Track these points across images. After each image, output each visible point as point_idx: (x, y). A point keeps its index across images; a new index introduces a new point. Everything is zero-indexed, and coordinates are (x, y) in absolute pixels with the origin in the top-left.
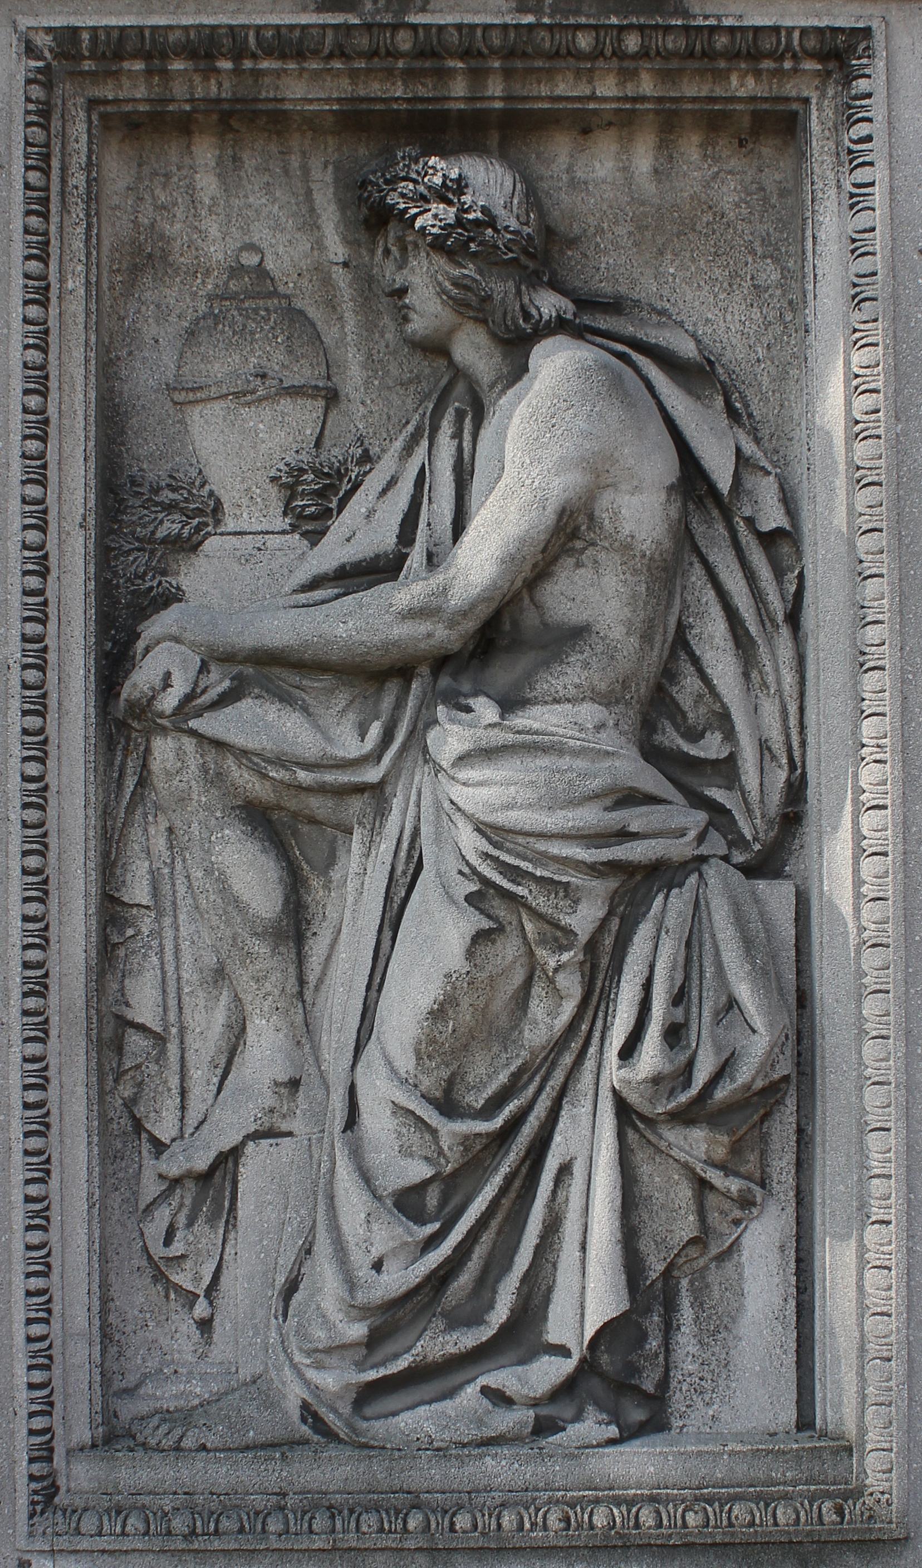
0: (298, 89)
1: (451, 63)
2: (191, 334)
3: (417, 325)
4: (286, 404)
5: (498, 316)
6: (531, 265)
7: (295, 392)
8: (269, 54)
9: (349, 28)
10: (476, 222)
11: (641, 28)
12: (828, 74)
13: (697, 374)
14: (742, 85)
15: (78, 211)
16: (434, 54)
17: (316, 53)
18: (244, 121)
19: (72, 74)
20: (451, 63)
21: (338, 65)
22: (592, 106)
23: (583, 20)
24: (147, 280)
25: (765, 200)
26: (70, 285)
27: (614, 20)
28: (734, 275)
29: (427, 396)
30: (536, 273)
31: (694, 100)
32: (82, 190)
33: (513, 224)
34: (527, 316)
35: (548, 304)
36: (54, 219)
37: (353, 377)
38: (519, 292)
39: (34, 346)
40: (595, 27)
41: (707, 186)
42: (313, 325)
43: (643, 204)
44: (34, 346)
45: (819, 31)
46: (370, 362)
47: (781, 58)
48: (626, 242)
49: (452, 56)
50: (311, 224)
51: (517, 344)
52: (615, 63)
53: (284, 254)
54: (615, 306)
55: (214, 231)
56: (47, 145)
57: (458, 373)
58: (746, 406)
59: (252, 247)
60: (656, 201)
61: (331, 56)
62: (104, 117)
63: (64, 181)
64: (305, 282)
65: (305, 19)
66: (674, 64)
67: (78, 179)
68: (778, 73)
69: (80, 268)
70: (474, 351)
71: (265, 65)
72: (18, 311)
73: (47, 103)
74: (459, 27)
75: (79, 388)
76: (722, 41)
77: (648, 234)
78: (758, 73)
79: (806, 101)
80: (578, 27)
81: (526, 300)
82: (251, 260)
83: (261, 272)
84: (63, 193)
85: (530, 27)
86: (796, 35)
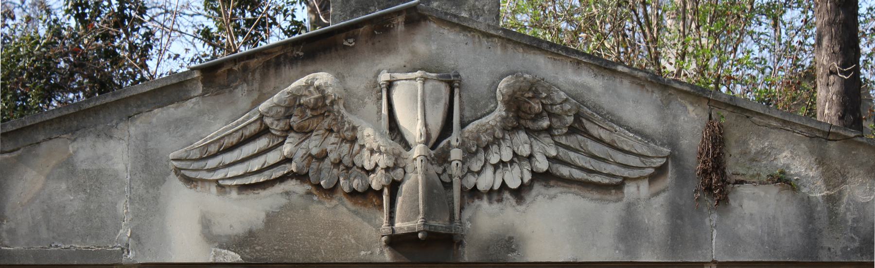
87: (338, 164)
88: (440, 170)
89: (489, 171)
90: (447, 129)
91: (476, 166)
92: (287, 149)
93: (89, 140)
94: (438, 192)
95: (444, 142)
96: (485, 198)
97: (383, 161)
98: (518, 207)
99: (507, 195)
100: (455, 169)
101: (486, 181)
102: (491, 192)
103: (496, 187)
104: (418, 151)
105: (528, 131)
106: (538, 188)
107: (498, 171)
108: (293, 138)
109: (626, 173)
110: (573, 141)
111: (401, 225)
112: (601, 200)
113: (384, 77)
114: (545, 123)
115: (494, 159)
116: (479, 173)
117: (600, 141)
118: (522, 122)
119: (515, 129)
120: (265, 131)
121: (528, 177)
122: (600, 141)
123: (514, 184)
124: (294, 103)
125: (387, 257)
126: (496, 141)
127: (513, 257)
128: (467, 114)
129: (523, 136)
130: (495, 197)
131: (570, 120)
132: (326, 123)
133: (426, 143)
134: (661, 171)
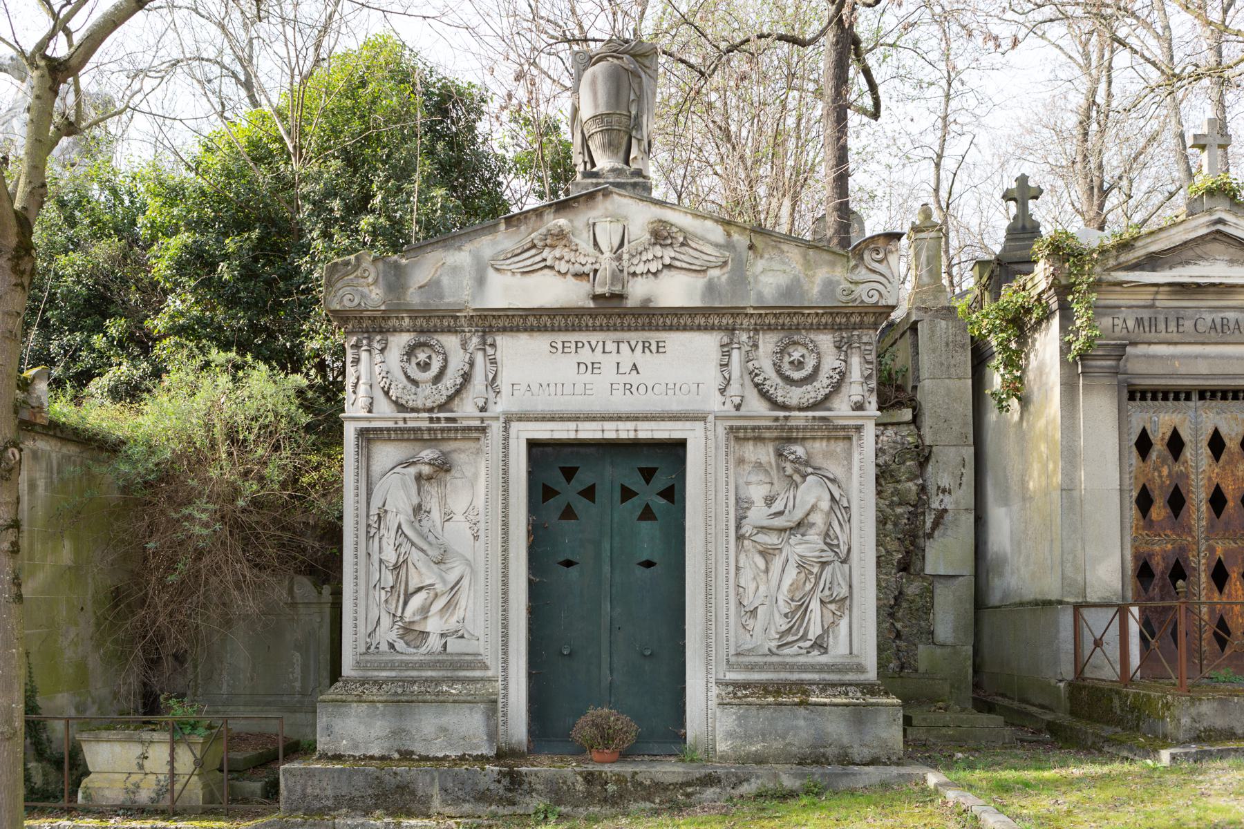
0: (767, 435)
18: (759, 439)
35: (810, 470)
37: (775, 481)
51: (804, 477)
54: (819, 469)
70: (797, 477)
87: (568, 262)
89: (642, 264)
90: (622, 244)
91: (635, 261)
92: (544, 255)
93: (451, 251)
94: (618, 275)
97: (591, 260)
100: (625, 263)
101: (641, 268)
104: (608, 254)
106: (665, 271)
108: (547, 250)
111: (599, 291)
113: (591, 221)
114: (669, 241)
115: (644, 258)
119: (655, 244)
120: (534, 246)
121: (660, 267)
123: (653, 270)
124: (549, 233)
125: (592, 305)
127: (652, 305)
128: (632, 238)
129: (658, 247)
131: (681, 239)
132: (564, 242)
134: (725, 263)
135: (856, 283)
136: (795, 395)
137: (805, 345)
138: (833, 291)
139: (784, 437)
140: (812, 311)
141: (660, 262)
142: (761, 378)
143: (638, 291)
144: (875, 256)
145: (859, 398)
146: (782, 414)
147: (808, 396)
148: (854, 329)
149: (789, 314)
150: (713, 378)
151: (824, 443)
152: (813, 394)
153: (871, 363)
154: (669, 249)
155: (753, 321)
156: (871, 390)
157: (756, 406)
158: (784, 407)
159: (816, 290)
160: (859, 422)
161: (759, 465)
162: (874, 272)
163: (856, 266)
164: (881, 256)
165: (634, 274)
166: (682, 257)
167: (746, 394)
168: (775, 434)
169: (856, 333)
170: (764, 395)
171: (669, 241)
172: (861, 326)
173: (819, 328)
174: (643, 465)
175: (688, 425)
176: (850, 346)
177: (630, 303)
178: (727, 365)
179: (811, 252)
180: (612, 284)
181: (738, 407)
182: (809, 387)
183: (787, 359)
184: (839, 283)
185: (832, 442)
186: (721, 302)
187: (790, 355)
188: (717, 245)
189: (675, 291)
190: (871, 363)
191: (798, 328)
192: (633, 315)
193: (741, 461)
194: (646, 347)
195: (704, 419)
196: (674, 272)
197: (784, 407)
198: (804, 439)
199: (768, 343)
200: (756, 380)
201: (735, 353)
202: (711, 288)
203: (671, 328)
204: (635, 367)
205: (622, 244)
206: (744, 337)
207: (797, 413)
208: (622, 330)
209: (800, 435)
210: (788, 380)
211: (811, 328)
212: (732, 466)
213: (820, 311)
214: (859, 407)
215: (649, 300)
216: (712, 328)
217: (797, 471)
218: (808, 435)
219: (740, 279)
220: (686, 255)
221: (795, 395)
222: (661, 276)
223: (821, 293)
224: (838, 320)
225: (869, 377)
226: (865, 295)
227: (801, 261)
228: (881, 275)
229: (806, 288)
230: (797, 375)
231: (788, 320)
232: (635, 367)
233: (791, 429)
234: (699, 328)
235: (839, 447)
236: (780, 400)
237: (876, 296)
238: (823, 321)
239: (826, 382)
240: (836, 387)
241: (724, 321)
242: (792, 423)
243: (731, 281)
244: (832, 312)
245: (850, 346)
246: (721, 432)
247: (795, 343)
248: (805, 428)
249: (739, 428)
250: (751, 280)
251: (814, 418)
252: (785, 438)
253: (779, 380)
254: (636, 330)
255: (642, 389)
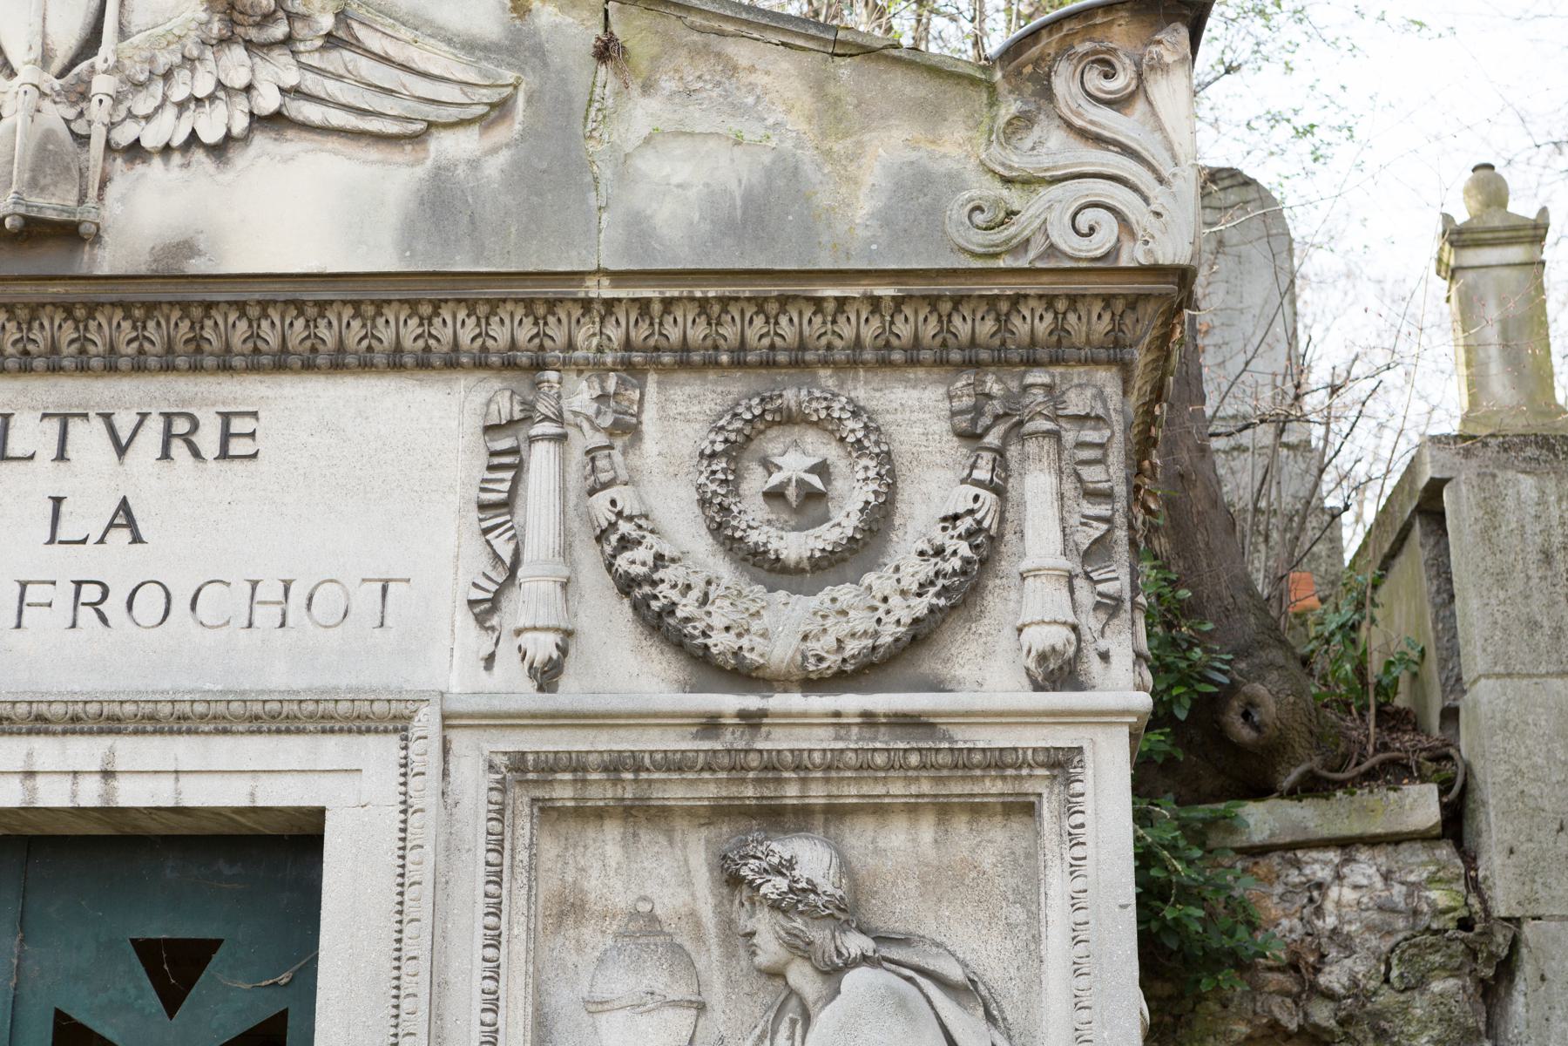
1: (786, 775)
2: (601, 960)
3: (762, 959)
4: (669, 1013)
5: (819, 954)
6: (843, 917)
7: (675, 1004)
8: (658, 768)
9: (715, 752)
10: (804, 890)
11: (920, 750)
12: (1055, 777)
13: (965, 991)
14: (993, 787)
15: (522, 878)
16: (774, 768)
17: (691, 768)
18: (641, 814)
19: (520, 782)
20: (786, 775)
21: (706, 775)
22: (887, 800)
23: (878, 745)
24: (570, 921)
25: (1015, 861)
26: (516, 931)
27: (902, 745)
28: (993, 916)
29: (770, 1007)
30: (847, 921)
31: (960, 796)
32: (525, 863)
33: (830, 890)
34: (839, 954)
35: (856, 943)
36: (505, 885)
37: (716, 994)
38: (834, 937)
39: (491, 978)
40: (888, 750)
41: (973, 851)
42: (689, 956)
43: (927, 865)
44: (491, 978)
45: (1047, 749)
46: (730, 982)
47: (1020, 767)
48: (914, 893)
49: (787, 770)
50: (687, 882)
51: (833, 973)
52: (902, 773)
53: (668, 901)
54: (905, 941)
55: (619, 886)
56: (502, 833)
57: (792, 992)
58: (1001, 1011)
59: (644, 899)
60: (936, 863)
61: (702, 769)
62: (541, 809)
63: (513, 858)
64: (683, 923)
65: (684, 746)
66: (945, 773)
67: (523, 856)
68: (1018, 778)
69: (523, 919)
70: (802, 977)
71: (656, 776)
72: (479, 952)
73: (502, 803)
74: (792, 751)
75: (520, 1005)
76: (977, 757)
77: (930, 888)
78: (1004, 778)
79: (1040, 795)
80: (875, 750)
81: (839, 942)
82: (644, 907)
83: (652, 918)
84: (512, 866)
85: (842, 751)
86: (1030, 753)
88: (71, 113)
89: (170, 112)
90: (91, 43)
91: (143, 104)
95: (83, 66)
96: (157, 162)
98: (220, 178)
99: (199, 155)
100: (98, 112)
101: (164, 129)
102: (167, 149)
103: (177, 142)
105: (249, 45)
106: (261, 141)
107: (186, 114)
109: (433, 113)
110: (337, 60)
112: (384, 162)
114: (279, 31)
115: (179, 93)
116: (148, 118)
117: (385, 60)
118: (239, 30)
121: (240, 124)
122: (385, 60)
123: (211, 135)
126: (189, 61)
127: (196, 266)
129: (238, 53)
130: (177, 158)
131: (327, 22)
133: (45, 59)
134: (501, 108)
135: (1028, 182)
136: (783, 627)
137: (827, 426)
138: (934, 211)
139: (754, 797)
140: (853, 291)
141: (242, 104)
142: (641, 553)
143: (143, 215)
144: (1095, 81)
145: (1058, 637)
146: (729, 702)
147: (837, 628)
148: (1032, 363)
149: (760, 303)
150: (449, 556)
151: (927, 831)
152: (860, 621)
153: (1108, 496)
154: (281, 57)
155: (615, 333)
156: (1110, 607)
157: (627, 673)
158: (743, 675)
159: (864, 207)
160: (1062, 738)
161: (645, 927)
162: (1099, 140)
163: (1024, 121)
164: (1122, 81)
165: (135, 151)
166: (332, 88)
167: (583, 623)
168: (709, 791)
169: (1037, 377)
170: (658, 624)
171: (279, 31)
172: (1056, 352)
173: (888, 360)
174: (156, 930)
175: (332, 749)
176: (1016, 431)
177: (107, 260)
178: (507, 505)
179: (845, 69)
180: (34, 184)
181: (547, 675)
182: (846, 593)
183: (755, 482)
184: (955, 182)
185: (960, 824)
186: (479, 252)
187: (768, 466)
188: (471, 47)
189: (295, 213)
190: (1108, 496)
191: (799, 362)
192: (126, 307)
193: (569, 909)
194: (177, 434)
195: (398, 724)
196: (295, 144)
197: (743, 675)
198: (836, 813)
199: (679, 421)
200: (622, 562)
201: (542, 459)
202: (440, 202)
203: (281, 363)
204: (125, 515)
205: (91, 43)
206: (581, 395)
207: (794, 701)
208: (83, 369)
209: (817, 794)
210: (762, 565)
211: (853, 361)
212: (516, 929)
213: (886, 291)
214: (1060, 672)
215: (187, 248)
216: (452, 363)
217: (800, 948)
218: (850, 793)
219: (559, 167)
220: (344, 83)
221: (783, 627)
222: (241, 159)
223: (885, 219)
224: (962, 328)
225: (1098, 551)
226: (1058, 223)
227: (807, 101)
228: (1126, 151)
229: (823, 199)
230: (794, 546)
231: (761, 322)
232: (125, 515)
233: (772, 767)
234: (396, 362)
235: (990, 845)
236: (720, 643)
237: (1108, 233)
238: (904, 330)
239: (916, 571)
240: (963, 590)
241: (500, 333)
242: (778, 741)
243: (524, 177)
244: (933, 291)
245: (1016, 431)
246: (472, 779)
247: (789, 419)
248: (832, 765)
249: (549, 767)
250: (605, 172)
251: (869, 719)
252: (757, 808)
253: (724, 570)
254: (139, 368)
255: (149, 603)
